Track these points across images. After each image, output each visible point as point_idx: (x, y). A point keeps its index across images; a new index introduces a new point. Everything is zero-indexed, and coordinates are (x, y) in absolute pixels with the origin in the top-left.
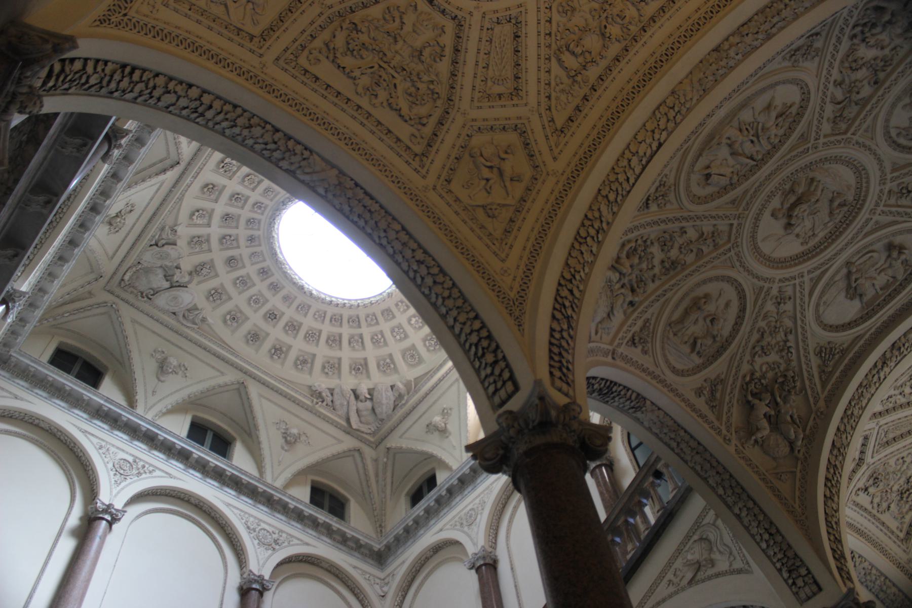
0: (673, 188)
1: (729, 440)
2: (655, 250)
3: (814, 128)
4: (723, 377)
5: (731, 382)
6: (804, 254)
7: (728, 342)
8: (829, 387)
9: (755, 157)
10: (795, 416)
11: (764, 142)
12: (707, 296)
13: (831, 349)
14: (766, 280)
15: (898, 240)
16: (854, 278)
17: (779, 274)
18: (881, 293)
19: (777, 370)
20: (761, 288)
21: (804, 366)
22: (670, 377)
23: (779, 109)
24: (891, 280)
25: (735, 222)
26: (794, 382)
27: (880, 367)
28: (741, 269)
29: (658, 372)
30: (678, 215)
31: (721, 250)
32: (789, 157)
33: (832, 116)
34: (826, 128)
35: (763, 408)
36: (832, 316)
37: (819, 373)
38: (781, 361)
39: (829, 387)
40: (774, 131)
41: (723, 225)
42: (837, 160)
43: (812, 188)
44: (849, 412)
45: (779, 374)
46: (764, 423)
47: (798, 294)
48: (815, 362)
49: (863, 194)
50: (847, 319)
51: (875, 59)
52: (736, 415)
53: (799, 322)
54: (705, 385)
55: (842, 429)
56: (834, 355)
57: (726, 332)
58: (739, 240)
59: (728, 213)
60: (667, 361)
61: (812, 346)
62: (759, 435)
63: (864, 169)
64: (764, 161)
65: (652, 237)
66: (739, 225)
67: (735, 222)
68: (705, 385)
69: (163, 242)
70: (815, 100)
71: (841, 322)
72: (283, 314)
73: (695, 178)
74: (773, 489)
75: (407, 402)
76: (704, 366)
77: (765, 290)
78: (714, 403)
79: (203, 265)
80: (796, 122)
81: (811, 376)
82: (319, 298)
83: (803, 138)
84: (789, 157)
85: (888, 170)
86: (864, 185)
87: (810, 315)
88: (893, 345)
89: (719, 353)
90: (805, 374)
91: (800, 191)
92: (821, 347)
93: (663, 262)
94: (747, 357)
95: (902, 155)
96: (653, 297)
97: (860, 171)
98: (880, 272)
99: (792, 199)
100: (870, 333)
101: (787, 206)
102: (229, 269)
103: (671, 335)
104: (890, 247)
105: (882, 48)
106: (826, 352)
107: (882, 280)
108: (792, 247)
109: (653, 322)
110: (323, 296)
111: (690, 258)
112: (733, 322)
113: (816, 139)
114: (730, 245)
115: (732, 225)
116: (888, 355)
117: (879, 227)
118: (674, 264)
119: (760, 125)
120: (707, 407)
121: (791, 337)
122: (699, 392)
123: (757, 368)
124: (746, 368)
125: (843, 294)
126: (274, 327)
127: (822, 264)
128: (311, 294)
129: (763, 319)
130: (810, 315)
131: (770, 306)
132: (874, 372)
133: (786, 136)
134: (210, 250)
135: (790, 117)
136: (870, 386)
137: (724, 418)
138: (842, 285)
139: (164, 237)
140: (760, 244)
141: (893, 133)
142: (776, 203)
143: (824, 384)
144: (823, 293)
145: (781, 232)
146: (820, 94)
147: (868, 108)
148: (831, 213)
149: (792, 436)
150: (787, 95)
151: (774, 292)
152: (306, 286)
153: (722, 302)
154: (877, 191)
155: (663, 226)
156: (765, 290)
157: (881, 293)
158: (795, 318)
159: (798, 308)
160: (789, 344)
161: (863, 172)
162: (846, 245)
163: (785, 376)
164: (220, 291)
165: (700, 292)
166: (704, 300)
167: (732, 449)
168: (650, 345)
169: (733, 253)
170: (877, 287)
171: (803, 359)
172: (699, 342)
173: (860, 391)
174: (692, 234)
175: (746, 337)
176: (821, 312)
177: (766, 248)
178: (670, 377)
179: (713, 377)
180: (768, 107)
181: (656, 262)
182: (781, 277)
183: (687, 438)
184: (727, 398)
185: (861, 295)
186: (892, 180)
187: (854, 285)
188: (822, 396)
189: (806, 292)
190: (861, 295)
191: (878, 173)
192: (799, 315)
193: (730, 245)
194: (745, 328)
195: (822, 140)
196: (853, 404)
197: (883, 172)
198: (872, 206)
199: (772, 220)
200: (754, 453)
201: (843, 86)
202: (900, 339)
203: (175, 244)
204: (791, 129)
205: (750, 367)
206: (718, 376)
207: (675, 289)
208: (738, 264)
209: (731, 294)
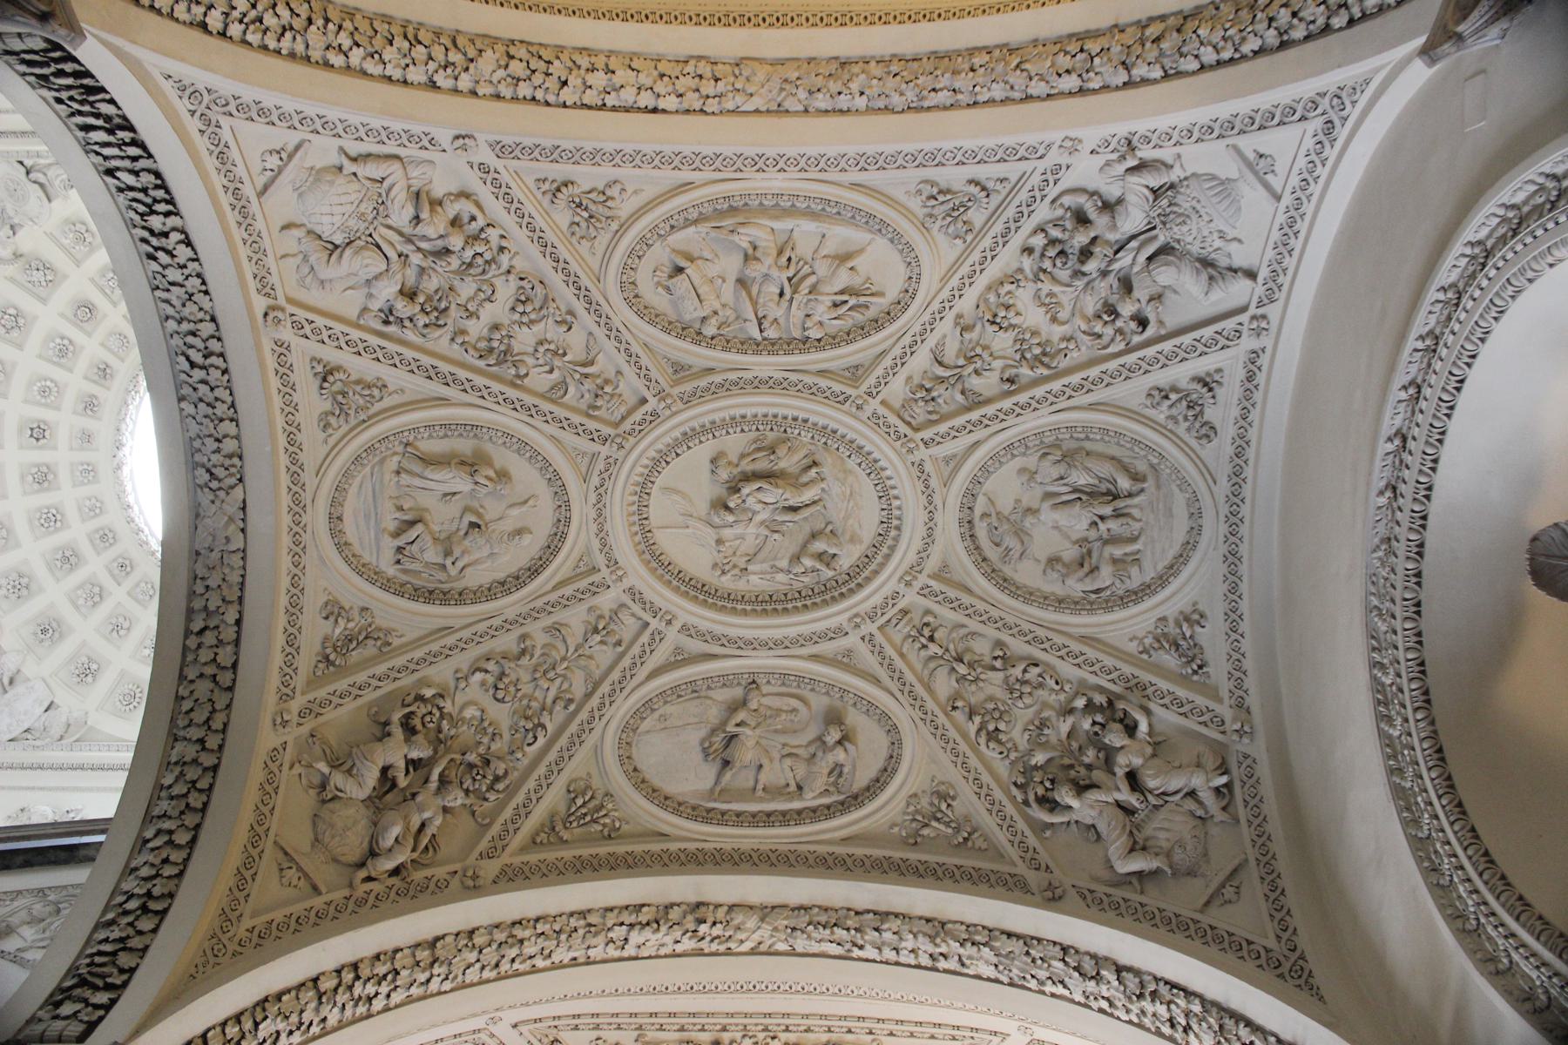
0: (615, 226)
1: (285, 723)
2: (506, 291)
3: (879, 371)
4: (396, 642)
5: (400, 661)
6: (702, 587)
7: (461, 597)
8: (533, 858)
9: (766, 324)
10: (429, 831)
11: (797, 314)
12: (503, 476)
13: (602, 806)
14: (613, 563)
15: (854, 718)
16: (741, 716)
17: (638, 574)
18: (760, 793)
19: (486, 740)
20: (594, 570)
21: (531, 784)
22: (317, 517)
23: (857, 281)
24: (793, 788)
25: (652, 403)
26: (491, 788)
27: (643, 918)
28: (593, 498)
29: (308, 477)
30: (585, 281)
31: (592, 425)
32: (809, 380)
33: (916, 381)
34: (897, 389)
35: (395, 752)
36: (653, 753)
37: (543, 825)
38: (506, 736)
39: (533, 858)
40: (822, 311)
41: (631, 385)
42: (873, 468)
43: (805, 479)
44: (519, 933)
45: (482, 750)
46: (371, 777)
47: (636, 650)
48: (554, 798)
49: (867, 573)
50: (671, 788)
51: (1034, 333)
52: (342, 717)
53: (595, 701)
54: (355, 614)
55: (479, 940)
56: (595, 821)
57: (476, 578)
58: (632, 440)
59: (654, 374)
60: (340, 489)
61: (576, 767)
62: (338, 779)
63: (898, 528)
64: (772, 346)
65: (519, 263)
66: (654, 414)
67: (652, 403)
68: (355, 614)
69: (42, 179)
70: (911, 318)
71: (656, 782)
72: (55, 448)
73: (660, 254)
74: (249, 863)
75: (42, 748)
76: (388, 585)
77: (596, 578)
78: (331, 659)
79: (46, 267)
80: (863, 330)
81: (525, 810)
82: (121, 484)
83: (855, 373)
84: (809, 380)
85: (932, 564)
86: (879, 559)
87: (624, 707)
88: (699, 905)
89: (429, 596)
90: (520, 798)
91: (782, 464)
92: (588, 787)
93: (496, 327)
94: (463, 660)
95: (967, 562)
96: (426, 361)
97: (890, 526)
98: (789, 755)
99: (762, 465)
100: (683, 845)
101: (747, 466)
102: (70, 314)
103: (393, 463)
104: (834, 718)
105: (1054, 320)
106: (586, 806)
107: (777, 773)
108: (692, 550)
109: (388, 402)
110: (129, 488)
111: (540, 380)
112: (501, 576)
113: (869, 394)
114: (612, 431)
115: (644, 401)
117: (844, 661)
118: (506, 356)
119: (813, 279)
120: (318, 647)
121: (560, 713)
122: (333, 611)
123: (460, 698)
124: (442, 672)
125: (703, 733)
126: (21, 447)
127: (716, 638)
128: (119, 467)
129: (547, 630)
130: (624, 707)
131: (575, 618)
132: (628, 918)
133: (834, 340)
134: (78, 263)
135: (863, 313)
136: (596, 934)
137: (321, 693)
138: (714, 714)
139: (50, 173)
140: (655, 490)
141: (980, 506)
142: (735, 443)
143: (534, 843)
144: (675, 692)
145: (702, 507)
146: (927, 317)
147: (975, 415)
148: (796, 558)
149: (388, 841)
150: (880, 265)
151: (606, 601)
152: (126, 450)
153: (515, 517)
154: (887, 590)
155: (546, 265)
156: (596, 578)
157: (760, 793)
158: (597, 685)
159: (615, 675)
160: (545, 719)
161: (893, 533)
162: (777, 644)
163: (487, 762)
164: (21, 321)
165: (504, 457)
166: (492, 474)
167: (268, 739)
168: (345, 428)
169: (605, 450)
170: (763, 778)
171: (542, 770)
172: (419, 528)
173: (573, 922)
174: (576, 342)
175: (496, 622)
176: (645, 726)
177: (660, 508)
178: (317, 517)
179: (379, 622)
180: (843, 258)
181: (489, 313)
182: (640, 585)
183: (229, 634)
184: (361, 677)
185: (726, 763)
186: (925, 592)
187: (731, 728)
188: (505, 858)
189: (653, 662)
190: (726, 763)
191: (912, 557)
192: (605, 688)
193: (612, 431)
194: (510, 605)
195: (874, 405)
196: (540, 928)
197: (920, 562)
198: (861, 609)
199: (707, 466)
200: (295, 801)
201: (967, 336)
202: (717, 906)
203: (49, 200)
204: (848, 336)
205: (452, 684)
206: (388, 632)
207: (471, 398)
208: (595, 481)
209: (542, 519)
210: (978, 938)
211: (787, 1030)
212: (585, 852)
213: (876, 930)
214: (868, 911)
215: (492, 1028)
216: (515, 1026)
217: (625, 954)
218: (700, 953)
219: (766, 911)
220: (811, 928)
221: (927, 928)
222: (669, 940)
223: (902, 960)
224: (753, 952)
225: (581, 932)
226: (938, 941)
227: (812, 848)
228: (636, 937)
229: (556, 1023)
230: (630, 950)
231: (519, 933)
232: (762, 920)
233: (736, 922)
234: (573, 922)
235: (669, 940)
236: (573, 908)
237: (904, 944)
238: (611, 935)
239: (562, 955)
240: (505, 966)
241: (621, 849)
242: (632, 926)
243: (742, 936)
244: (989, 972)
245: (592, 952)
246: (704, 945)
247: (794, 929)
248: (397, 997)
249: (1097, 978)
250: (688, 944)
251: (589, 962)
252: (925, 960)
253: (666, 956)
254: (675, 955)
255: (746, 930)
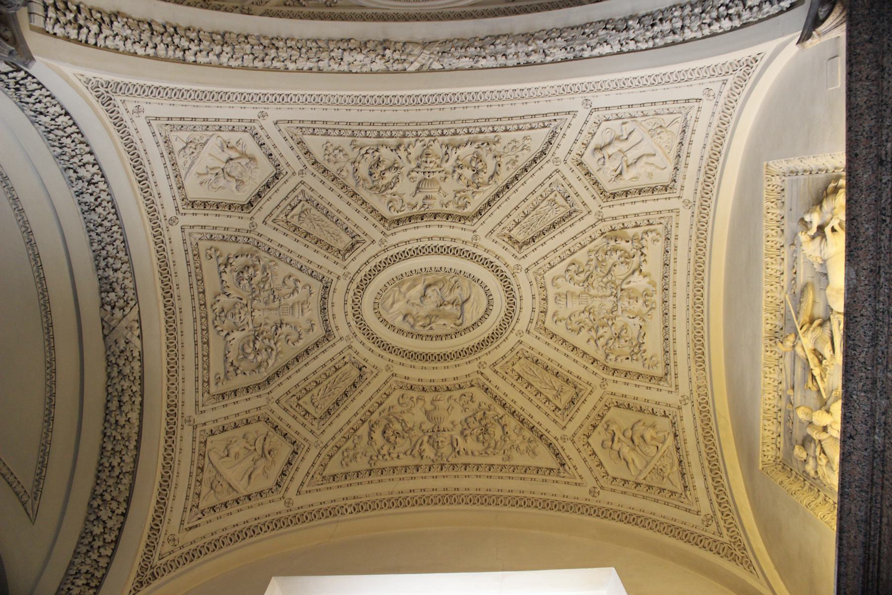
88: (385, 41)
100: (374, 11)
116: (370, 45)
173: (309, 44)
210: (554, 35)
211: (443, 135)
212: (316, 11)
213: (493, 44)
214: (487, 37)
215: (263, 123)
216: (276, 123)
217: (342, 68)
218: (387, 71)
219: (425, 45)
220: (453, 49)
221: (524, 39)
222: (367, 61)
223: (510, 63)
224: (418, 71)
225: (314, 50)
226: (530, 42)
227: (452, 10)
228: (347, 57)
229: (301, 125)
230: (344, 67)
231: (278, 44)
232: (424, 48)
233: (407, 51)
234: (309, 44)
235: (367, 61)
236: (309, 36)
237: (509, 51)
238: (332, 54)
239: (303, 64)
240: (268, 63)
241: (337, 11)
242: (344, 50)
243: (411, 59)
244: (561, 54)
245: (321, 64)
246: (389, 64)
247: (444, 52)
248: (201, 58)
249: (627, 29)
250: (379, 65)
251: (320, 71)
252: (523, 59)
253: (366, 73)
254: (371, 72)
255: (414, 55)
